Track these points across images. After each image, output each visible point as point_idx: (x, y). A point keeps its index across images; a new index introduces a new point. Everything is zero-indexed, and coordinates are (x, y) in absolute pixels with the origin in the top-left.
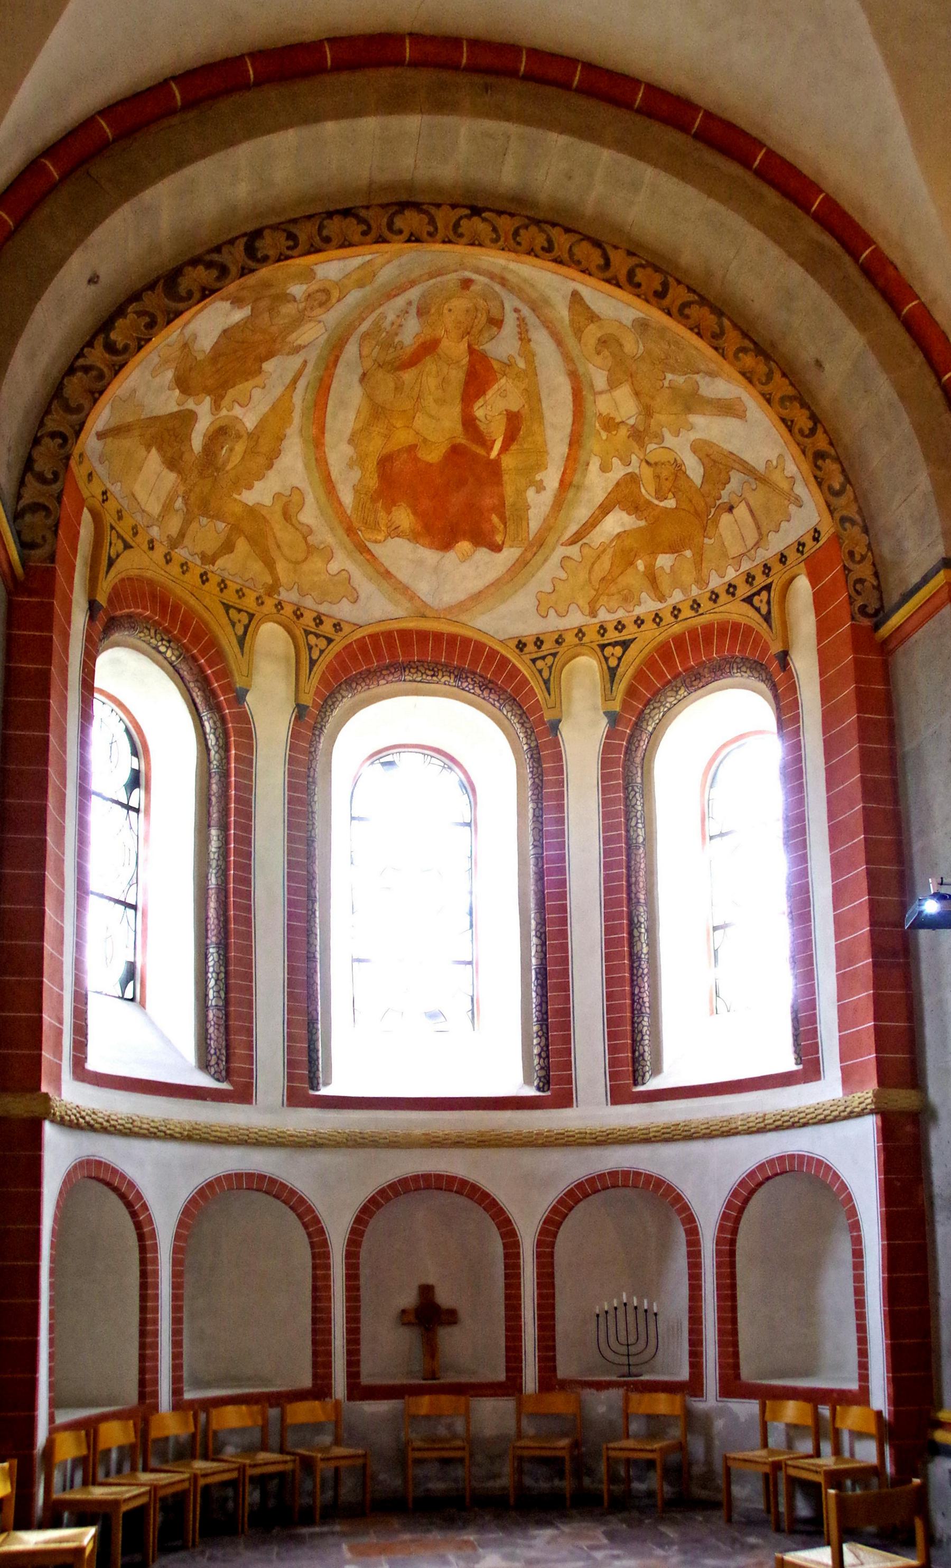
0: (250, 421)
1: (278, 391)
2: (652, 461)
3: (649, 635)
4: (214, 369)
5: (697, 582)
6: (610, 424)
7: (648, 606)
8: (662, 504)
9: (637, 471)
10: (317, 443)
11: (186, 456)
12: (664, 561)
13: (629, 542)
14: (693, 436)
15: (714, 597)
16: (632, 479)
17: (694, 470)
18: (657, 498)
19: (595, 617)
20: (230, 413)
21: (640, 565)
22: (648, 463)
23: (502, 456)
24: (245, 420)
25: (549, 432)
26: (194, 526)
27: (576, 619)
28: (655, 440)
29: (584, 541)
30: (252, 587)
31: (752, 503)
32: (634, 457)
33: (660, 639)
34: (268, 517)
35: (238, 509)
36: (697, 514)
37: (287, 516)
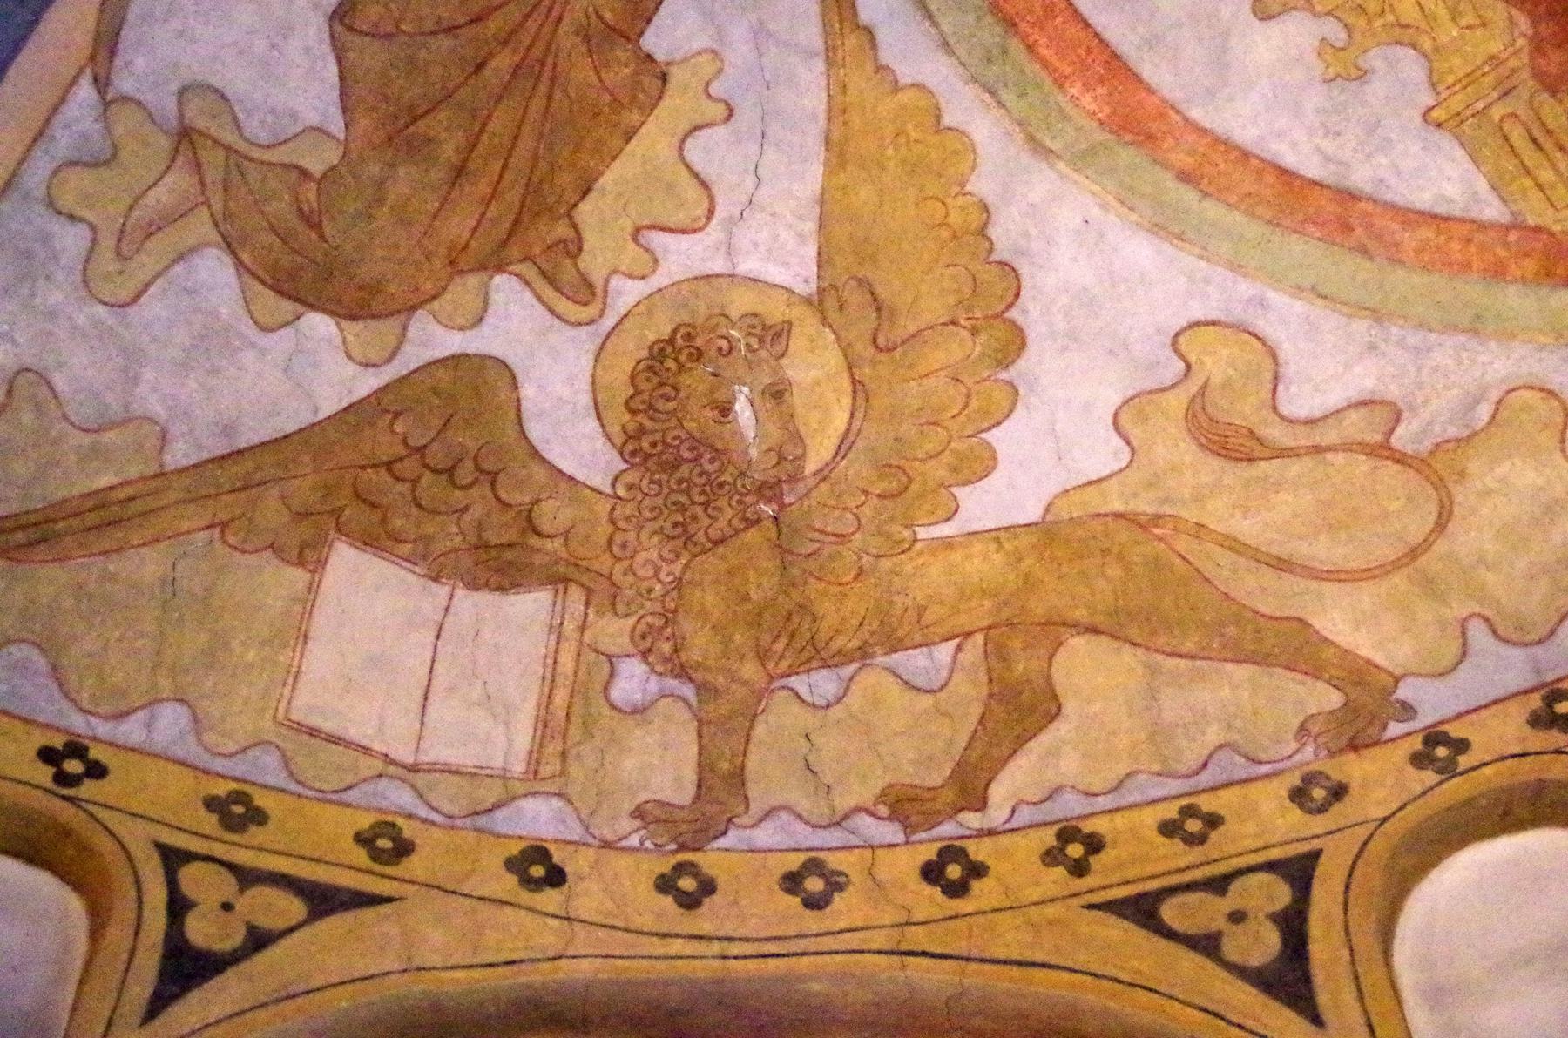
0: (775, 250)
1: (808, 92)
4: (438, 174)
10: (1135, 122)
11: (554, 514)
20: (659, 280)
24: (748, 265)
26: (781, 719)
30: (1241, 769)
34: (1144, 505)
35: (982, 565)
37: (1228, 444)
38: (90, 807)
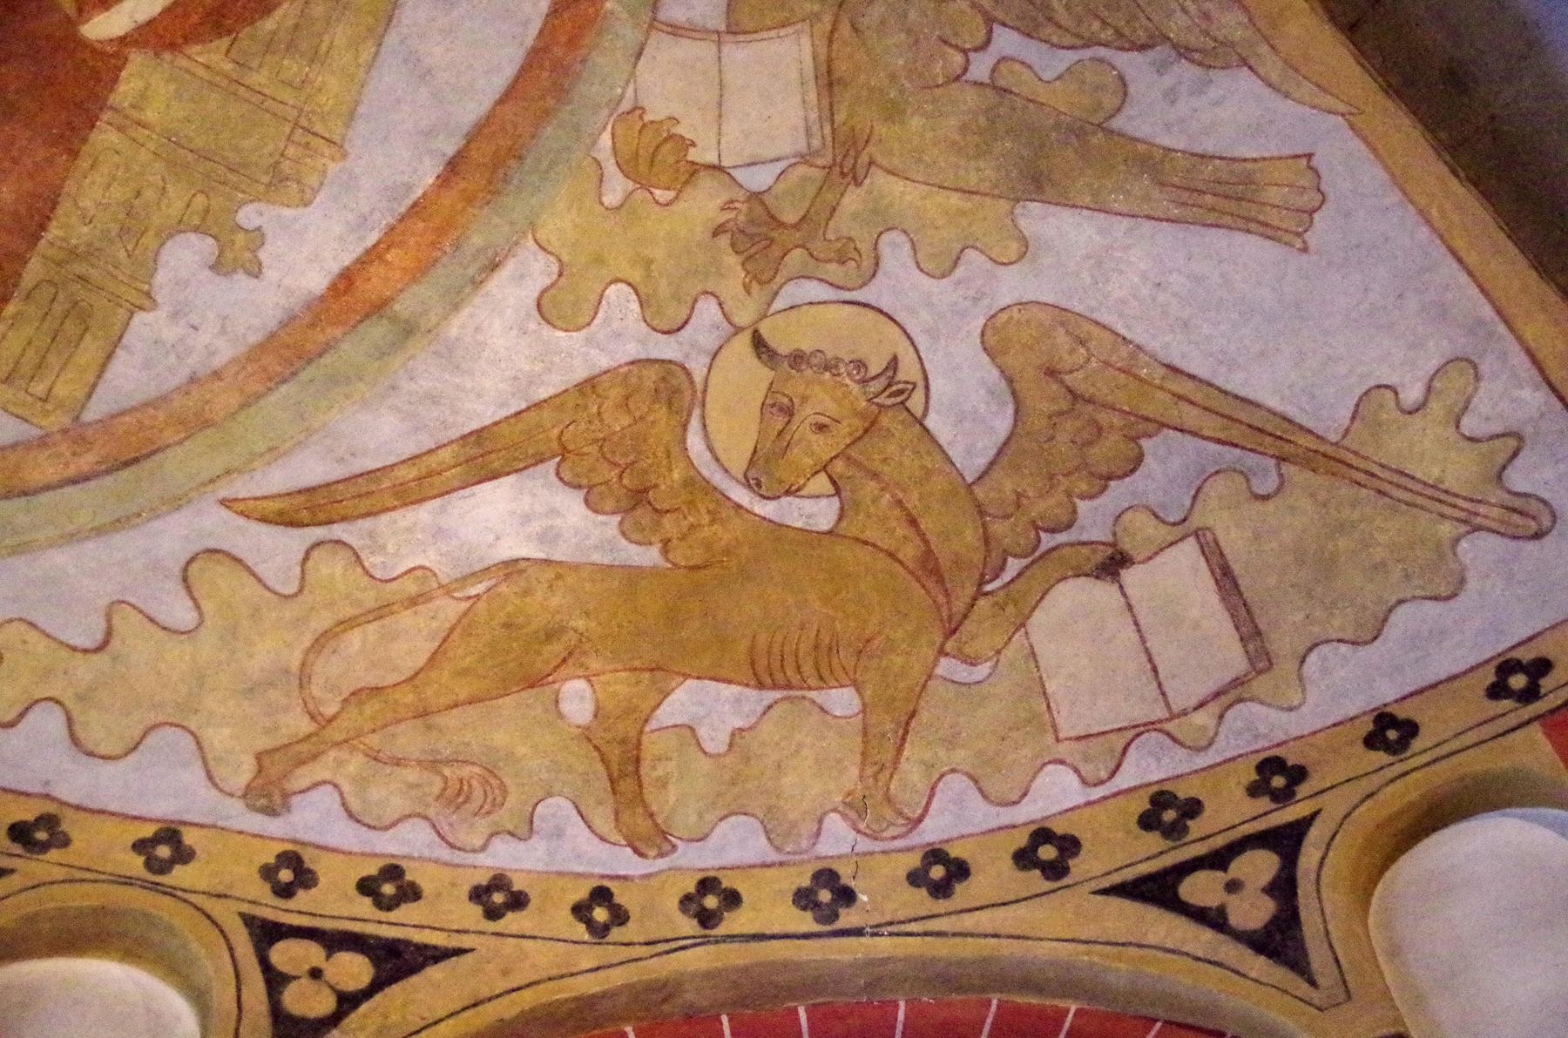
2: (782, 338)
3: (542, 957)
5: (855, 809)
6: (660, 159)
7: (566, 847)
8: (766, 509)
9: (698, 368)
12: (708, 707)
13: (547, 603)
14: (1012, 286)
15: (943, 872)
16: (672, 389)
17: (966, 413)
18: (752, 484)
19: (270, 811)
21: (577, 699)
22: (759, 343)
23: (137, 60)
25: (389, 77)
27: (164, 787)
28: (833, 270)
29: (338, 531)
31: (1234, 542)
32: (708, 311)
33: (590, 985)
36: (930, 568)
38: (192, 898)
